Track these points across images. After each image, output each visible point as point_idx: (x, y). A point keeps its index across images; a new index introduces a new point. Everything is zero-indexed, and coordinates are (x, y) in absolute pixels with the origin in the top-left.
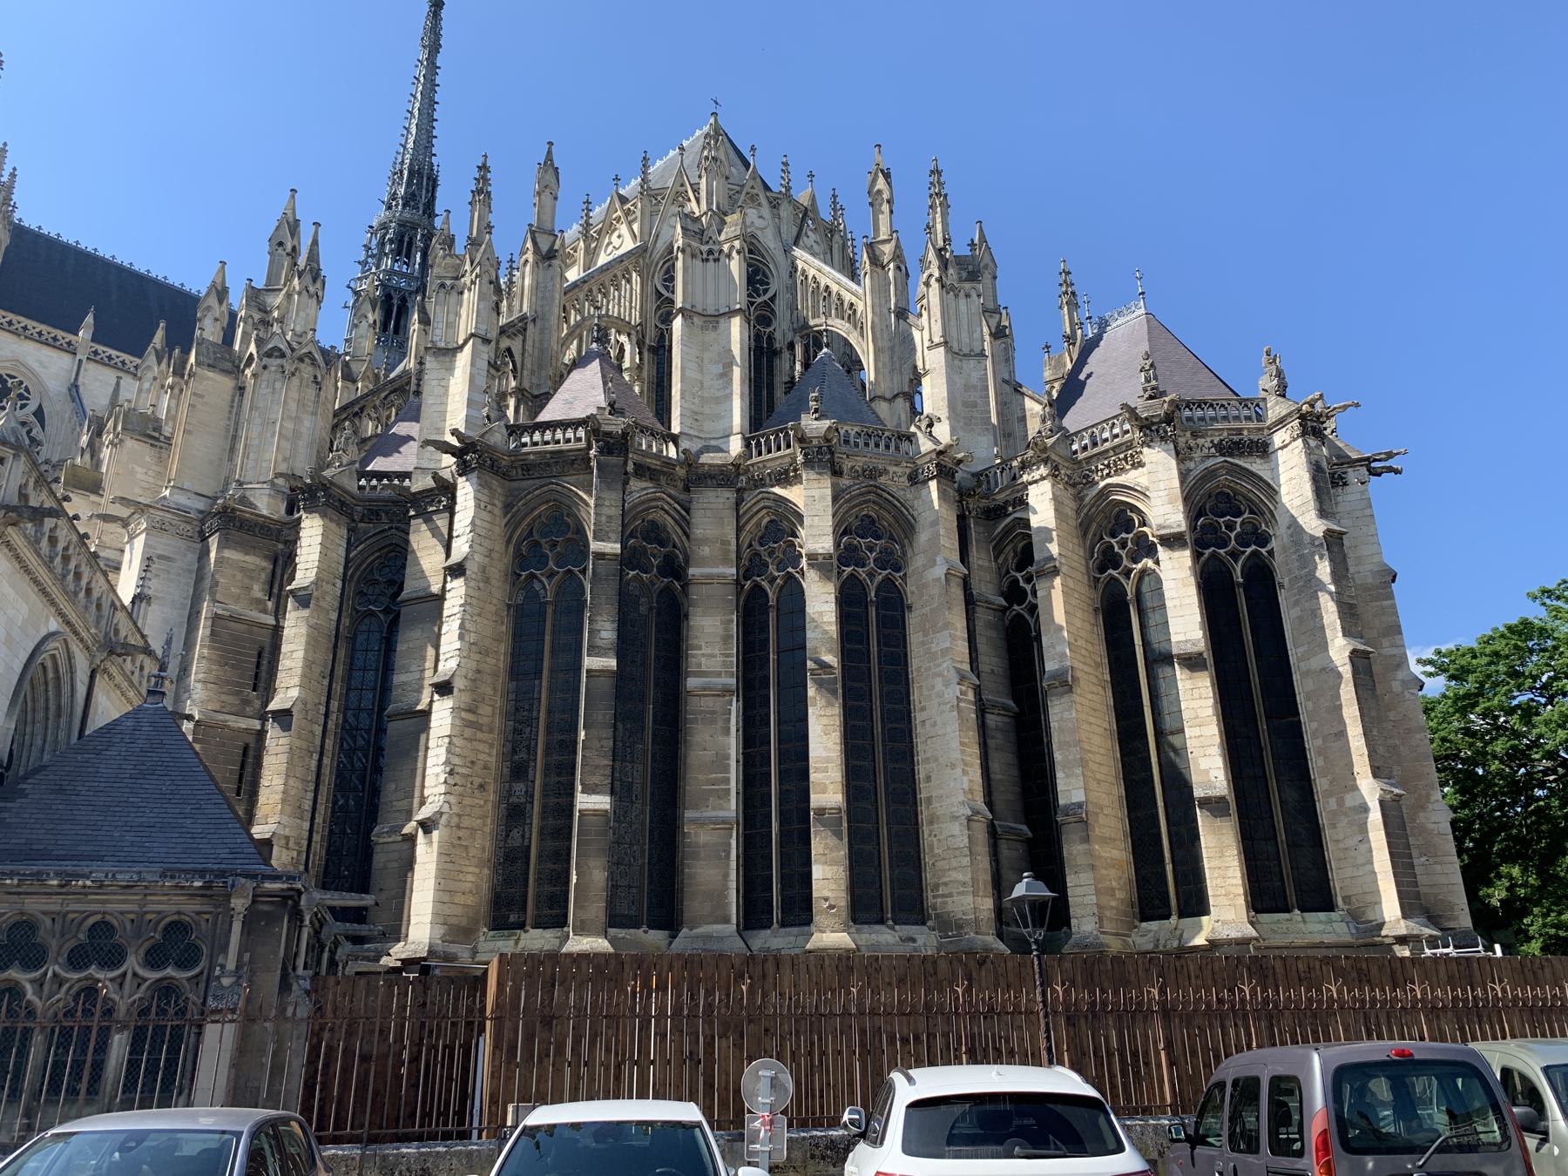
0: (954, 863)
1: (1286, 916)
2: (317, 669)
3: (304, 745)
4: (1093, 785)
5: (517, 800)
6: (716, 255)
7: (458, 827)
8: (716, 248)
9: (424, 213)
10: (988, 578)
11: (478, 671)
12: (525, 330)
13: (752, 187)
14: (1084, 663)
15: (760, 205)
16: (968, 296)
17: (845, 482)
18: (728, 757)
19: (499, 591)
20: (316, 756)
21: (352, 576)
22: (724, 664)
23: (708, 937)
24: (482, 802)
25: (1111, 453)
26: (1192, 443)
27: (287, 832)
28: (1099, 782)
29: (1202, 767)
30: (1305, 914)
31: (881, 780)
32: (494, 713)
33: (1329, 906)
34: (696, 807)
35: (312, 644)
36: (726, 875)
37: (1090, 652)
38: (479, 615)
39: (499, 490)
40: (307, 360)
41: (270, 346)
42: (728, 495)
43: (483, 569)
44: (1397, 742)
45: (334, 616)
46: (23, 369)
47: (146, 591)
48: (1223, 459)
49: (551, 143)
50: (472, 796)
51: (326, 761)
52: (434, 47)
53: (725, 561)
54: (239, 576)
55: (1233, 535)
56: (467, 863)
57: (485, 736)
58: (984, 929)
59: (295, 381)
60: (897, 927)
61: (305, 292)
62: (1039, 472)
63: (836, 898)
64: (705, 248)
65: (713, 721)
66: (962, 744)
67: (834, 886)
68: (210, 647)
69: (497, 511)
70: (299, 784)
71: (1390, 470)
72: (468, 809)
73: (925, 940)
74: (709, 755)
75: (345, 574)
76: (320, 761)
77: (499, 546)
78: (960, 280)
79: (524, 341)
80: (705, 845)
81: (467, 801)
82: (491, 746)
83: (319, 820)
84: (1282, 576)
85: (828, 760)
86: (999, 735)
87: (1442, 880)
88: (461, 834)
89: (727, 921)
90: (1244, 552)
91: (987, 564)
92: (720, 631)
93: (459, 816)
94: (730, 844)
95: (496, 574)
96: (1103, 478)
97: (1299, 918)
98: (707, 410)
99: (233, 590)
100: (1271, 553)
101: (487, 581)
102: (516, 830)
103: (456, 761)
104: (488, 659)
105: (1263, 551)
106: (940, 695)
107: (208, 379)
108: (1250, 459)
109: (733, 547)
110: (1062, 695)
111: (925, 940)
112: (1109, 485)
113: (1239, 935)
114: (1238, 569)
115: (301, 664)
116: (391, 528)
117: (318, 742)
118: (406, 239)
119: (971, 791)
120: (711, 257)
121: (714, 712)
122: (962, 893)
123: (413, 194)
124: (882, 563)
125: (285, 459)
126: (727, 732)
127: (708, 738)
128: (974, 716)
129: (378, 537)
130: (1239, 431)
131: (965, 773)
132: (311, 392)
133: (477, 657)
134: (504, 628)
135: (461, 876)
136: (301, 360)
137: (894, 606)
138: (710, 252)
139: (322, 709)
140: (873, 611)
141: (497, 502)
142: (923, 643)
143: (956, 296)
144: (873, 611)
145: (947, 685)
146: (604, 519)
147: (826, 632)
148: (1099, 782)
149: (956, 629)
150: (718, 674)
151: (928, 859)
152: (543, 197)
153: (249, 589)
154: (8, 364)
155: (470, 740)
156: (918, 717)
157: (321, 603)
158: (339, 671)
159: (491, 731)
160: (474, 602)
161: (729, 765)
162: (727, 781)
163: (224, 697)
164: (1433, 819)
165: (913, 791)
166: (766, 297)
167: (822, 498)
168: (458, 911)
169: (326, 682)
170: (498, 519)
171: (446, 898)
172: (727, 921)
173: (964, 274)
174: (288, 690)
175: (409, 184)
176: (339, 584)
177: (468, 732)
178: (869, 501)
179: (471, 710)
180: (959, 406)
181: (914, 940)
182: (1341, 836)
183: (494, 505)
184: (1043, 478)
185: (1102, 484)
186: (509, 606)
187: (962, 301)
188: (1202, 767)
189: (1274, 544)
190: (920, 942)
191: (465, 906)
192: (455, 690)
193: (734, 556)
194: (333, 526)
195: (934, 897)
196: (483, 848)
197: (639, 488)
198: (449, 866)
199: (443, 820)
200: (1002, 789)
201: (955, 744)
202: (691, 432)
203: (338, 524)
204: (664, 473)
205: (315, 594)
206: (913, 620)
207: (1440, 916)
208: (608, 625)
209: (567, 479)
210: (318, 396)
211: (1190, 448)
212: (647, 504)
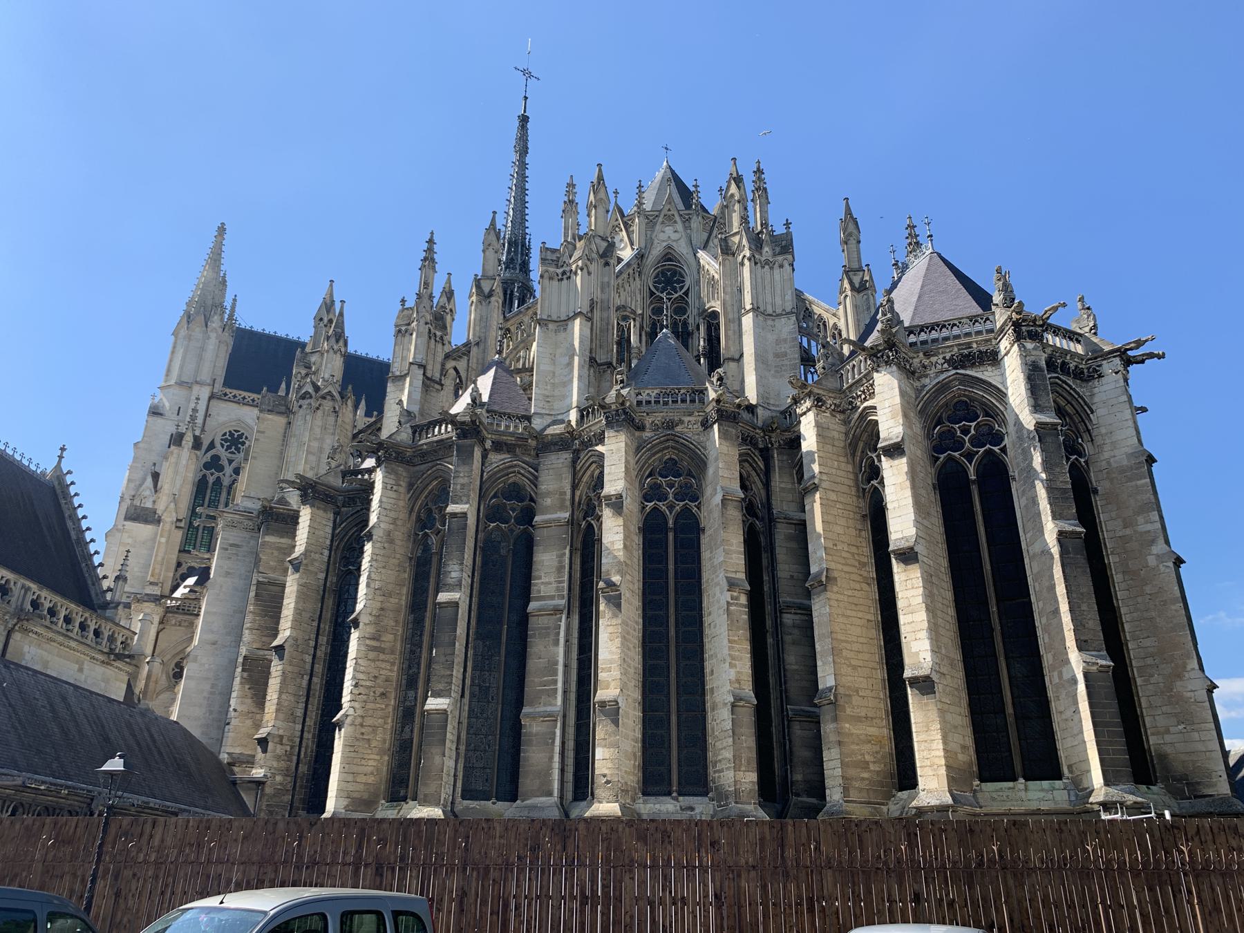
0: (725, 744)
1: (1011, 784)
2: (306, 615)
3: (296, 670)
4: (845, 670)
5: (409, 704)
6: (568, 274)
7: (362, 725)
8: (568, 269)
9: (521, 270)
10: (790, 497)
11: (382, 609)
12: (469, 352)
13: (669, 210)
14: (846, 564)
15: (675, 222)
16: (781, 266)
17: (647, 434)
18: (556, 663)
19: (402, 548)
20: (306, 678)
22: (558, 589)
23: (533, 807)
24: (384, 706)
25: (865, 381)
26: (926, 362)
27: (281, 732)
28: (855, 668)
29: (913, 650)
30: (1029, 783)
31: (673, 675)
32: (395, 640)
33: (1059, 776)
34: (531, 704)
35: (301, 596)
36: (551, 758)
37: (853, 554)
38: (384, 567)
39: (404, 474)
40: (328, 397)
41: (303, 392)
42: (566, 456)
43: (389, 533)
44: (1153, 614)
45: (322, 576)
46: (243, 425)
47: (123, 573)
48: (954, 372)
49: (495, 213)
50: (374, 702)
52: (523, 149)
53: (562, 508)
54: (276, 553)
55: (967, 439)
56: (370, 752)
57: (387, 657)
58: (744, 799)
59: (319, 413)
60: (681, 798)
61: (331, 351)
62: (805, 405)
63: (611, 775)
64: (560, 271)
65: (548, 635)
66: (730, 641)
67: (610, 765)
68: (255, 605)
69: (402, 490)
70: (292, 698)
71: (1151, 356)
72: (371, 712)
73: (702, 808)
74: (542, 662)
75: (331, 545)
77: (403, 515)
78: (775, 255)
79: (468, 360)
80: (537, 734)
81: (370, 706)
82: (393, 664)
83: (309, 722)
84: (1014, 471)
85: (611, 661)
86: (796, 631)
87: (1200, 747)
88: (363, 730)
89: (550, 794)
90: (978, 452)
91: (790, 486)
92: (556, 564)
93: (362, 717)
94: (555, 733)
95: (399, 536)
96: (862, 402)
97: (1022, 787)
98: (557, 393)
99: (272, 563)
100: (1004, 450)
101: (391, 541)
102: (408, 726)
103: (361, 676)
104: (391, 600)
105: (996, 449)
106: (718, 602)
107: (268, 420)
108: (982, 369)
109: (568, 496)
110: (819, 594)
111: (702, 808)
112: (865, 408)
113: (938, 802)
114: (972, 469)
115: (292, 613)
116: (362, 509)
117: (308, 667)
118: (509, 292)
119: (738, 681)
120: (565, 277)
121: (548, 628)
122: (728, 769)
123: (512, 259)
124: (679, 496)
125: (312, 469)
126: (557, 643)
127: (542, 648)
128: (746, 617)
129: (355, 516)
130: (969, 345)
131: (731, 666)
132: (331, 419)
133: (381, 599)
134: (406, 575)
135: (363, 762)
136: (324, 398)
137: (690, 530)
138: (564, 273)
139: (312, 643)
140: (671, 536)
141: (402, 483)
142: (710, 559)
143: (771, 268)
144: (671, 536)
145: (721, 593)
146: (459, 487)
147: (615, 557)
148: (855, 668)
149: (732, 545)
150: (552, 598)
151: (710, 740)
152: (487, 253)
154: (233, 423)
155: (373, 661)
156: (707, 620)
157: (310, 568)
158: (328, 615)
159: (392, 652)
160: (379, 558)
161: (557, 669)
162: (555, 682)
163: (264, 639)
164: (1190, 688)
165: (703, 684)
166: (681, 293)
167: (619, 450)
168: (362, 787)
169: (315, 624)
170: (402, 496)
171: (350, 778)
172: (550, 794)
173: (778, 249)
174: (285, 631)
175: (509, 252)
176: (326, 553)
177: (372, 655)
178: (667, 448)
179: (374, 638)
180: (771, 357)
181: (692, 809)
182: (1062, 709)
183: (399, 485)
184: (809, 410)
185: (862, 407)
186: (411, 559)
187: (777, 271)
188: (913, 650)
189: (1006, 441)
190: (697, 811)
191: (366, 784)
192: (361, 624)
193: (568, 503)
194: (321, 513)
195: (715, 772)
196: (384, 741)
197: (496, 459)
198: (353, 755)
199: (349, 720)
200: (797, 677)
201: (726, 642)
202: (543, 411)
203: (325, 511)
204: (520, 446)
205: (304, 562)
206: (704, 540)
207: (1198, 783)
208: (456, 567)
209: (447, 460)
210: (336, 421)
211: (925, 367)
212: (506, 471)
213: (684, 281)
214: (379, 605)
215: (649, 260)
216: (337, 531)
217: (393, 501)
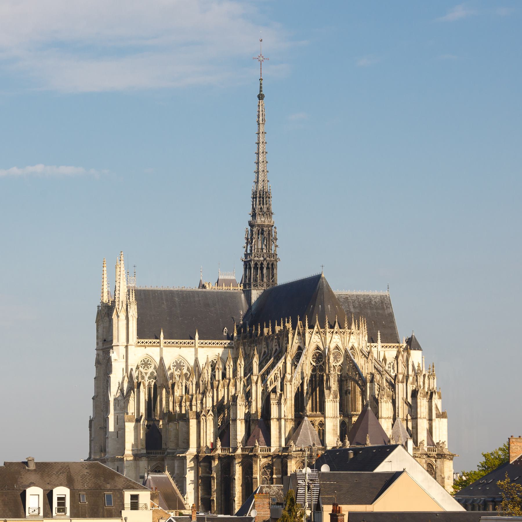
21: (223, 470)
51: (222, 506)
75: (221, 470)
76: (221, 506)
109: (281, 471)
117: (220, 503)
134: (244, 487)
139: (220, 497)
146: (255, 471)
153: (206, 470)
169: (220, 492)
173: (334, 396)
176: (220, 472)
193: (281, 473)
202: (274, 446)
213: (322, 358)
214: (239, 495)
215: (310, 350)
216: (222, 466)
217: (239, 469)
